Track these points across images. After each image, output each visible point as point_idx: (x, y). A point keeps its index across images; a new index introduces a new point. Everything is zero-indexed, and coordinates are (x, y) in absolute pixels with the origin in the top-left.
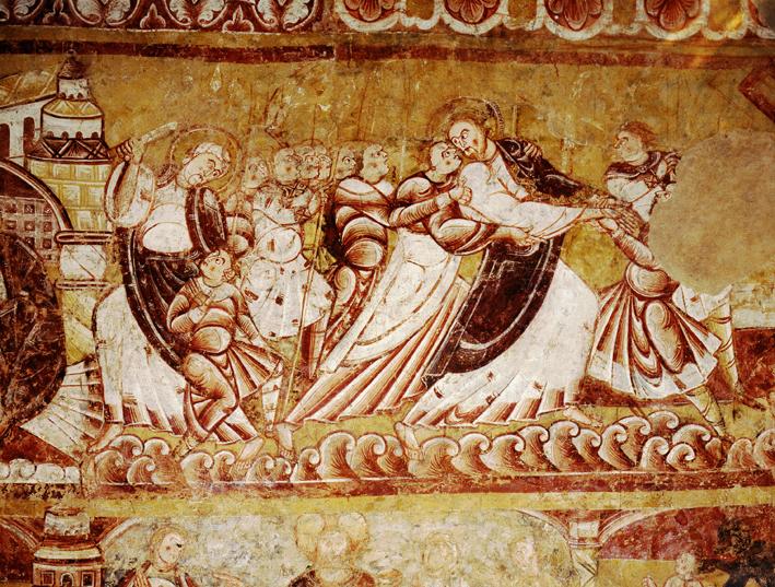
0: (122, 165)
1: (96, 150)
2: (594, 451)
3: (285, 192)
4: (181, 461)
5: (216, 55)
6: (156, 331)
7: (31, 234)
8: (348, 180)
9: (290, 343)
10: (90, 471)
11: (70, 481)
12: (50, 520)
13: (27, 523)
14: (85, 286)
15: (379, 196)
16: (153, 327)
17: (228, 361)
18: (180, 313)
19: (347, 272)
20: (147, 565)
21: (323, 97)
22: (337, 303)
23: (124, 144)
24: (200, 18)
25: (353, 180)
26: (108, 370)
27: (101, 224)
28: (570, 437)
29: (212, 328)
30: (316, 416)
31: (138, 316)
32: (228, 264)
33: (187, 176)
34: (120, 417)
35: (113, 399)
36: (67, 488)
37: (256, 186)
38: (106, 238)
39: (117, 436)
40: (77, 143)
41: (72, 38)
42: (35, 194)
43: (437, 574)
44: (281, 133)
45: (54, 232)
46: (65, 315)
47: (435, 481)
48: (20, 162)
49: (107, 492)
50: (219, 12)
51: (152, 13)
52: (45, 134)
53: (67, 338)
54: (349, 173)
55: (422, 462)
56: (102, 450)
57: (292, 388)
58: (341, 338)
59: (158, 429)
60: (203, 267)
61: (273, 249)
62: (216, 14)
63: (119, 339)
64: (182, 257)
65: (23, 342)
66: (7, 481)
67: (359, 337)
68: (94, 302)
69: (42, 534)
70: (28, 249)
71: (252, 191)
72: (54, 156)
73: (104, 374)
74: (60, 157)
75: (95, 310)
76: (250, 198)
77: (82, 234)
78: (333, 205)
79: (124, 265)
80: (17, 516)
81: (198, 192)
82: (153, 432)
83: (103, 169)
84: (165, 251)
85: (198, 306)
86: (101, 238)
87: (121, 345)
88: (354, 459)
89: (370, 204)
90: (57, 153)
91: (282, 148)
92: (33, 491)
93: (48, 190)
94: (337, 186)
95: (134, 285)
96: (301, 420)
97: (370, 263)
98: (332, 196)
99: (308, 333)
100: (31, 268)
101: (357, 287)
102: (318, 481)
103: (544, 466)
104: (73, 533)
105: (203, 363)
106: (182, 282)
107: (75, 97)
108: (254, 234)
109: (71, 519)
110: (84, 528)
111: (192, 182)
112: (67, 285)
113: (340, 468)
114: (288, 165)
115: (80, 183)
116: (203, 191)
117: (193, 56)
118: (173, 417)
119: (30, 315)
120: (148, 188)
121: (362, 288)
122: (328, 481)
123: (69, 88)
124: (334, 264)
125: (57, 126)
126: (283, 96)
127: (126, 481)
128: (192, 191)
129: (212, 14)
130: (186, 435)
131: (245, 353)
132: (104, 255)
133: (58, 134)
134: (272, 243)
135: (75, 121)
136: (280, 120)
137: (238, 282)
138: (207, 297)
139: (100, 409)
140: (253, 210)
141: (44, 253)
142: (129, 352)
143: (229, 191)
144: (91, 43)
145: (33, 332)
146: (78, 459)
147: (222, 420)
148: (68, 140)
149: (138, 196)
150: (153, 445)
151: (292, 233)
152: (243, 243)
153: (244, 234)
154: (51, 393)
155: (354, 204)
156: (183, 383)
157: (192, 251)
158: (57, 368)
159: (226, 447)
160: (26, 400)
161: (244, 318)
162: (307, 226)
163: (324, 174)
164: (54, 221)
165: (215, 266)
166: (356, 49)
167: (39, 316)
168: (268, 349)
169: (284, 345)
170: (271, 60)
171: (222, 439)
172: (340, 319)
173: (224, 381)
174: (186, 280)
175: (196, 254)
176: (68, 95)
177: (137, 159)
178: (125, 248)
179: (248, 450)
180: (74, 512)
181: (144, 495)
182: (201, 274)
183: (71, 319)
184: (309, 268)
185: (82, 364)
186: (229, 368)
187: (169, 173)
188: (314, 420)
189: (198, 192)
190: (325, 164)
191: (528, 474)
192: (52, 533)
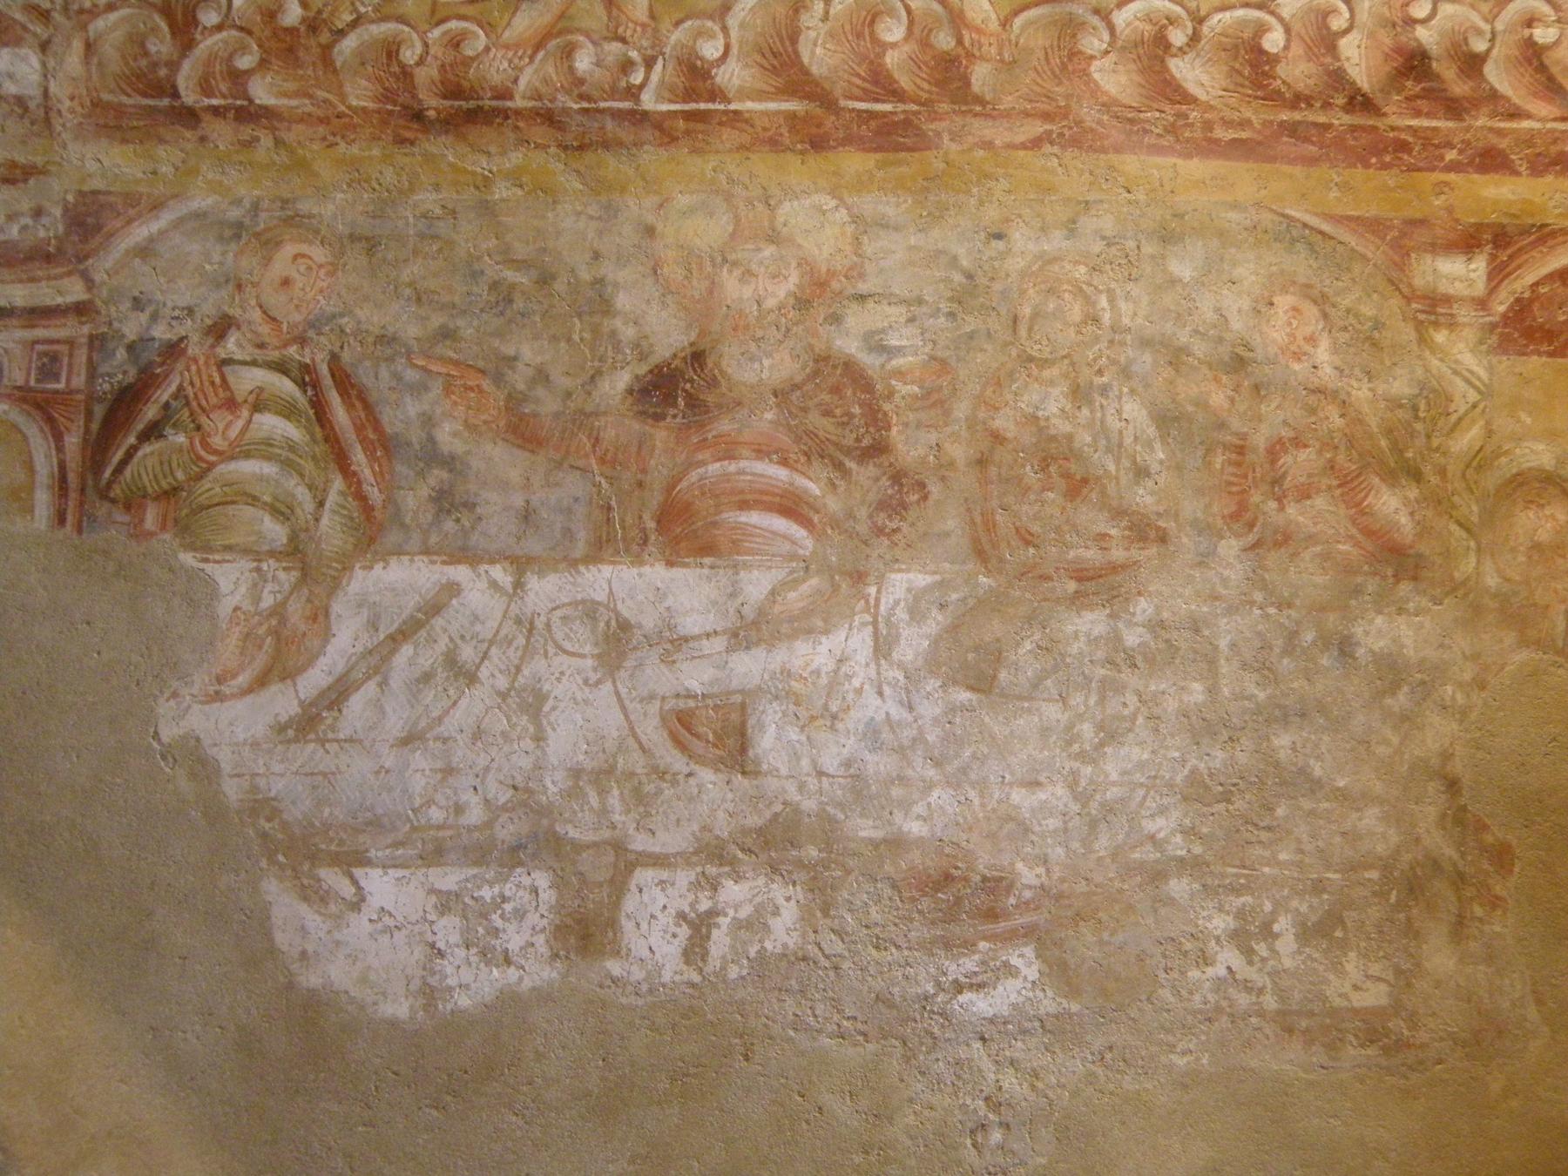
2: (1472, 64)
4: (335, 42)
10: (73, 61)
20: (220, 328)
28: (1411, 22)
43: (1054, 372)
47: (1047, 117)
49: (108, 121)
55: (1008, 66)
88: (820, 54)
102: (722, 107)
103: (1340, 100)
110: (45, 220)
113: (774, 71)
122: (749, 105)
127: (175, 94)
181: (222, 133)
191: (1297, 116)
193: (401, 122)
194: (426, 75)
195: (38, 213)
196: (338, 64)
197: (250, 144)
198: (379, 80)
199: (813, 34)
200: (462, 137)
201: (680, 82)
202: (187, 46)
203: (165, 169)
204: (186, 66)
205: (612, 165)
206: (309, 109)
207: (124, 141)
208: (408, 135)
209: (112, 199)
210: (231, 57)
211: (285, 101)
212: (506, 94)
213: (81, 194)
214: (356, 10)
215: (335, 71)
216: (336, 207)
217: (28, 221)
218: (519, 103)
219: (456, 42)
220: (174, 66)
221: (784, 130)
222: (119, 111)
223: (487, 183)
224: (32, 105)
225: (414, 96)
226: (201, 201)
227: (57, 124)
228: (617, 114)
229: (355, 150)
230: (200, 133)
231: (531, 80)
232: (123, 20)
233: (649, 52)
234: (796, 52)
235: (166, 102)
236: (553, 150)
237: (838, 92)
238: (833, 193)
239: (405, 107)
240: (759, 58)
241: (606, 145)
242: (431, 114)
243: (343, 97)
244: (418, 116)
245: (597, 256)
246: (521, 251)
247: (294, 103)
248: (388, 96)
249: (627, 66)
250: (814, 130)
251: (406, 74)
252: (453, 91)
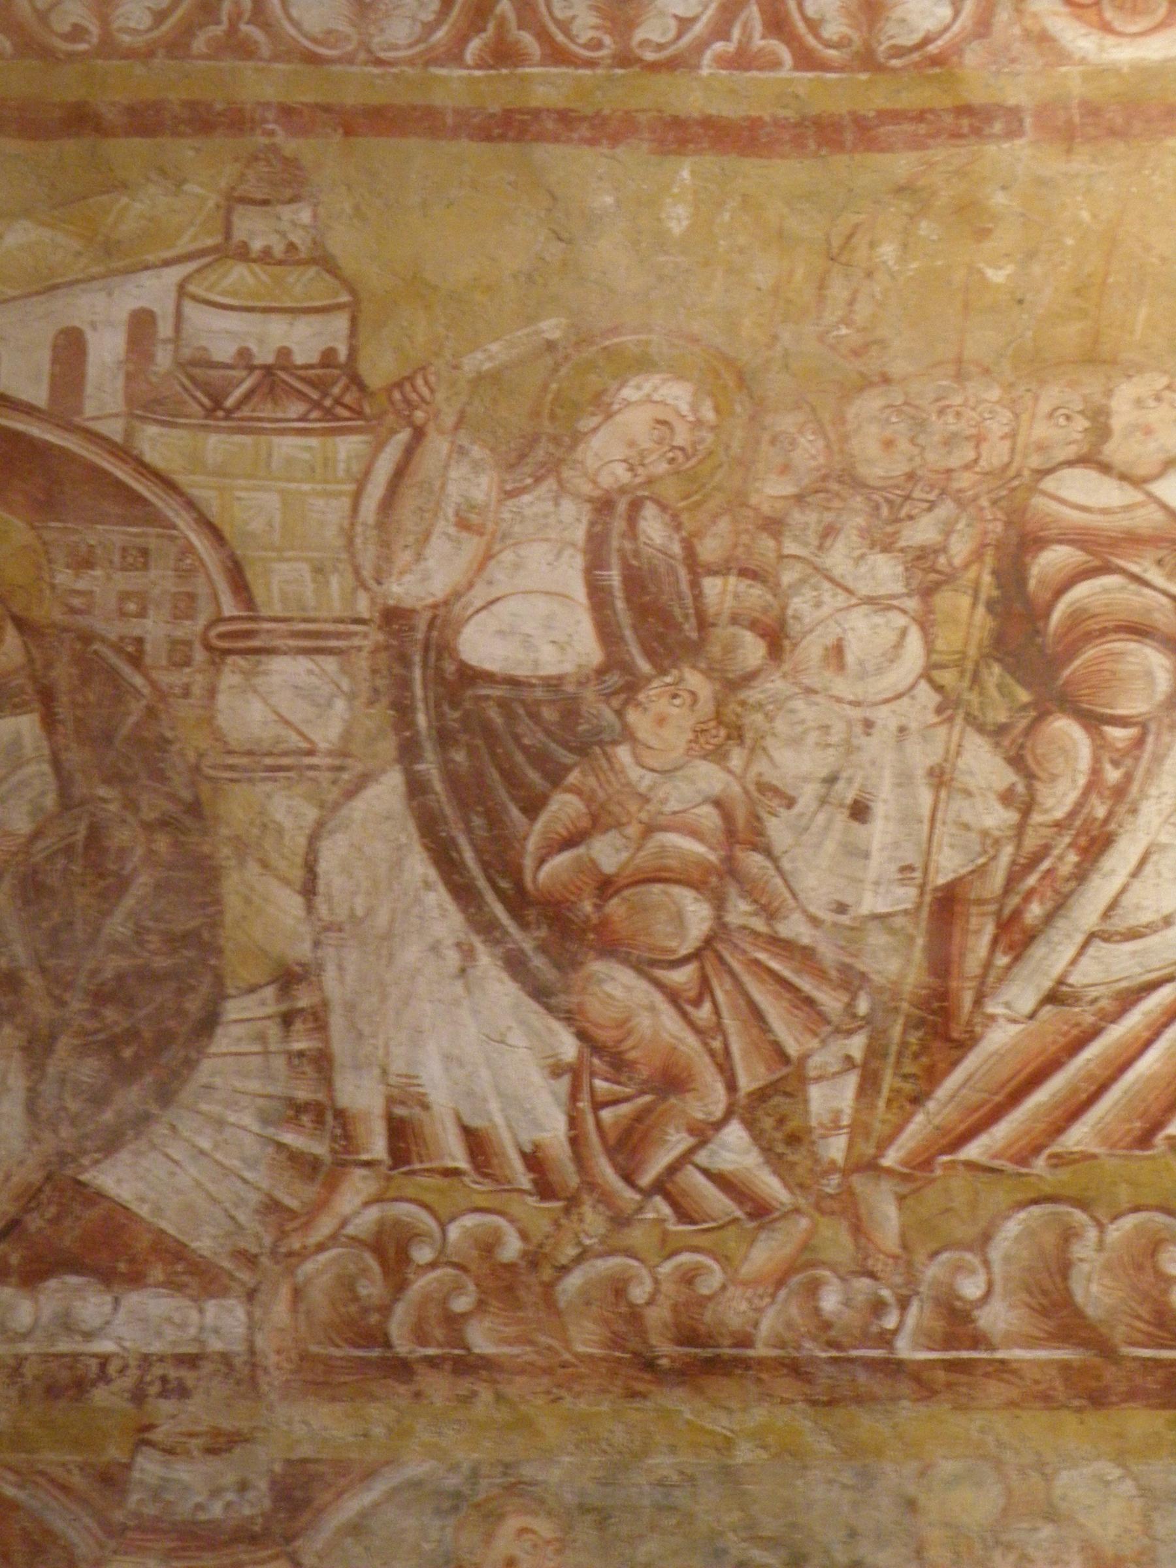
0: (404, 436)
1: (333, 393)
3: (877, 507)
4: (559, 1279)
5: (679, 134)
6: (490, 897)
7: (135, 628)
8: (1066, 472)
9: (892, 931)
10: (280, 1310)
11: (216, 1345)
12: (148, 1467)
13: (76, 1480)
14: (287, 768)
15: (1159, 516)
16: (482, 883)
17: (705, 984)
18: (570, 842)
19: (1065, 727)
21: (987, 245)
22: (1037, 818)
23: (410, 379)
24: (640, 35)
25: (1078, 472)
26: (350, 1008)
27: (336, 596)
29: (657, 888)
30: (973, 1151)
31: (444, 857)
32: (706, 707)
33: (591, 463)
34: (378, 1147)
35: (361, 1095)
36: (207, 1367)
37: (791, 490)
38: (349, 635)
39: (366, 1204)
40: (274, 378)
41: (271, 93)
42: (154, 518)
44: (867, 346)
45: (202, 621)
46: (226, 851)
48: (114, 429)
49: (318, 1378)
50: (693, 20)
51: (502, 23)
52: (186, 353)
53: (229, 918)
54: (1071, 452)
56: (321, 1247)
57: (898, 1063)
58: (1049, 919)
59: (488, 1186)
60: (632, 716)
61: (841, 667)
62: (685, 23)
63: (382, 918)
64: (570, 688)
65: (98, 930)
66: (27, 1348)
67: (1106, 915)
68: (311, 814)
69: (118, 1516)
70: (126, 669)
71: (779, 505)
72: (210, 413)
73: (337, 1022)
74: (226, 418)
75: (314, 839)
76: (774, 526)
77: (282, 626)
78: (1025, 541)
79: (403, 711)
80: (49, 1457)
81: (622, 506)
82: (478, 1189)
83: (348, 447)
84: (521, 672)
85: (619, 825)
86: (338, 635)
87: (388, 936)
88: (1095, 1291)
89: (1134, 540)
90: (218, 404)
91: (871, 384)
92: (103, 1376)
93: (190, 504)
94: (1032, 489)
95: (429, 766)
96: (927, 1164)
97: (1133, 706)
98: (1015, 516)
99: (947, 906)
100: (132, 720)
101: (1096, 772)
104: (216, 1510)
105: (628, 989)
106: (568, 758)
107: (278, 250)
108: (782, 622)
109: (214, 1464)
110: (250, 1495)
111: (606, 481)
112: (232, 768)
113: (1044, 1312)
114: (888, 433)
115: (283, 494)
116: (636, 506)
117: (615, 139)
118: (537, 1146)
119: (123, 853)
120: (479, 496)
121: (1113, 775)
123: (256, 230)
124: (1025, 707)
125: (221, 333)
126: (872, 245)
127: (387, 1344)
128: (604, 506)
129: (673, 24)
130: (572, 1202)
131: (757, 962)
132: (345, 684)
133: (224, 352)
134: (836, 653)
135: (273, 316)
136: (863, 311)
137: (737, 759)
138: (645, 799)
139: (319, 1121)
140: (781, 557)
141: (170, 679)
142: (411, 954)
143: (712, 505)
144: (327, 109)
145: (129, 902)
146: (244, 1275)
147: (686, 1158)
148: (251, 368)
149: (445, 525)
150: (467, 1232)
151: (900, 620)
152: (753, 650)
153: (753, 625)
154: (175, 1074)
155: (1081, 539)
156: (569, 1048)
157: (601, 672)
158: (193, 1005)
159: (703, 1241)
160: (99, 1099)
161: (754, 861)
162: (944, 600)
163: (995, 454)
164: (201, 587)
165: (666, 715)
166: (1092, 110)
167: (151, 856)
168: (828, 954)
169: (877, 939)
170: (838, 146)
171: (684, 1216)
172: (1045, 865)
173: (692, 1040)
174: (582, 750)
175: (615, 679)
176: (257, 245)
177: (449, 420)
178: (404, 660)
179: (765, 1253)
180: (221, 1444)
181: (438, 1387)
182: (628, 735)
183: (242, 864)
184: (950, 719)
185: (269, 992)
186: (707, 1006)
187: (540, 454)
188: (970, 1165)
189: (622, 506)
190: (997, 426)
192: (151, 1510)
193: (632, 1372)
194: (658, 1316)
195: (243, 1486)
196: (562, 1304)
197: (468, 1399)
198: (606, 1322)
199: (1086, 1267)
200: (699, 1390)
201: (939, 1325)
202: (400, 1287)
203: (378, 1431)
204: (400, 1310)
205: (868, 1424)
206: (533, 1357)
207: (333, 1399)
208: (640, 1387)
209: (321, 1468)
210: (445, 1300)
211: (506, 1350)
212: (745, 1341)
213: (289, 1462)
214: (579, 1244)
215: (558, 1313)
216: (562, 1472)
217: (230, 1496)
218: (760, 1351)
219: (688, 1278)
220: (386, 1311)
221: (1058, 1384)
222: (328, 1364)
223: (727, 1445)
224: (238, 1362)
225: (645, 1342)
226: (416, 1468)
227: (263, 1380)
228: (871, 1365)
229: (582, 1405)
230: (414, 1387)
231: (772, 1324)
232: (335, 1260)
233: (904, 1292)
234: (1068, 1290)
235: (376, 1353)
236: (800, 1405)
237: (1119, 1334)
238: (1120, 1458)
239: (636, 1354)
240: (1025, 1296)
241: (858, 1400)
242: (664, 1362)
243: (567, 1343)
244: (649, 1365)
245: (853, 1534)
246: (770, 1527)
247: (515, 1350)
248: (616, 1341)
249: (878, 1307)
250: (1094, 1384)
251: (635, 1316)
252: (688, 1336)
